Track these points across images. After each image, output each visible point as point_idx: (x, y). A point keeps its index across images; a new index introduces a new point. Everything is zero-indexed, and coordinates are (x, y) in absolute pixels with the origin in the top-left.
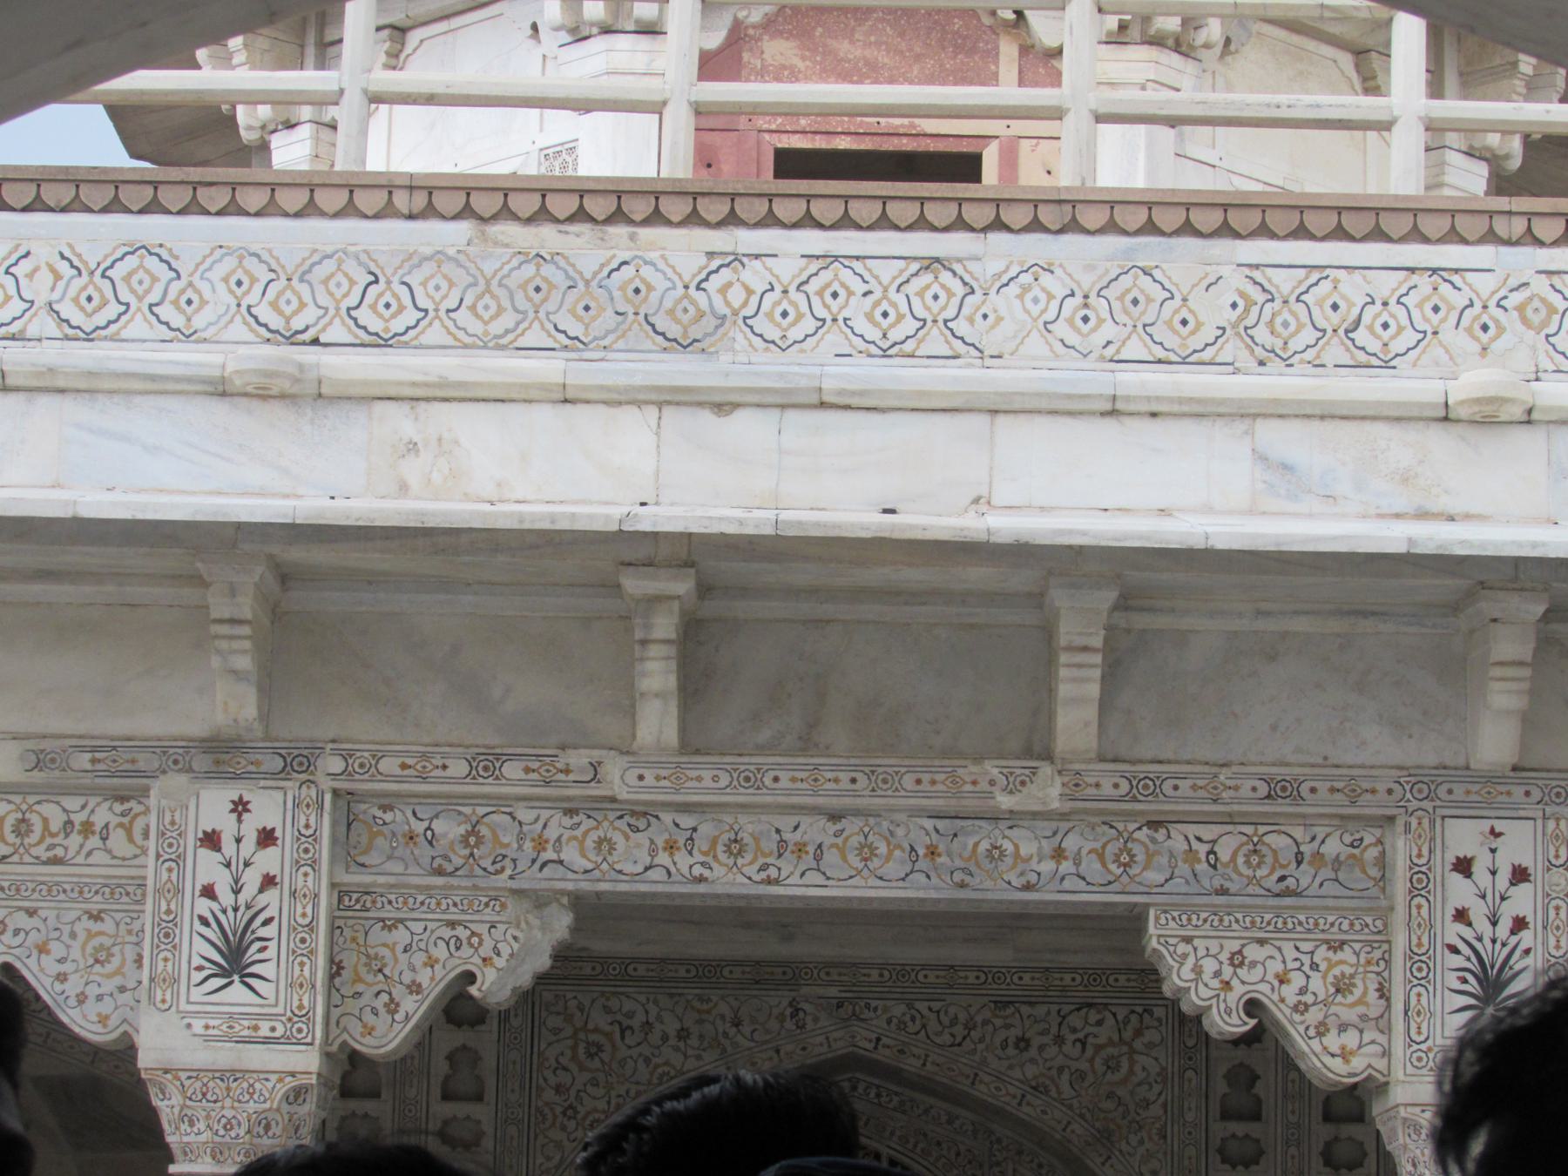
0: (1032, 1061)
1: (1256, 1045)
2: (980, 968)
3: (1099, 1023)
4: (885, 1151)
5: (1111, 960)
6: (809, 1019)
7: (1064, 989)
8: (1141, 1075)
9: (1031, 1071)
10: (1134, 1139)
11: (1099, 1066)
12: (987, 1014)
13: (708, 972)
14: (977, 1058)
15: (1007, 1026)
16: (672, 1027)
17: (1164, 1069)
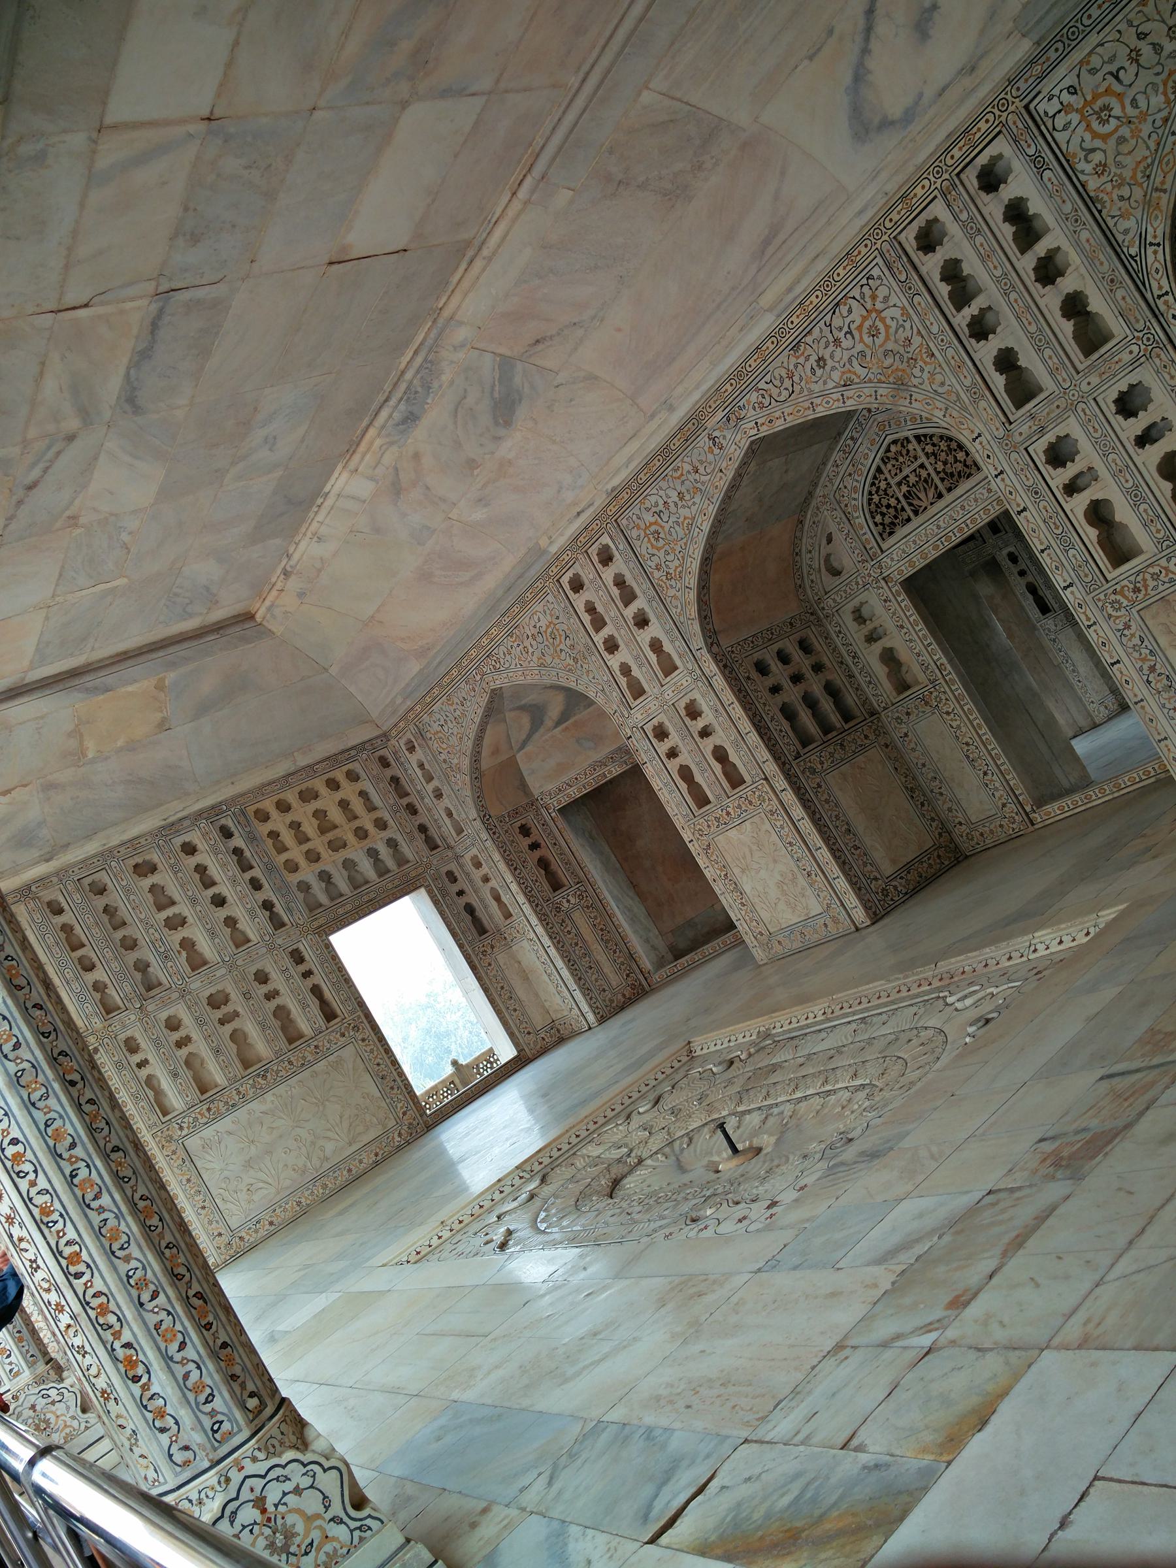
0: (833, 368)
1: (945, 240)
2: (770, 336)
3: (850, 311)
4: (909, 434)
5: (823, 265)
6: (722, 441)
7: (816, 308)
8: (893, 324)
9: (836, 375)
10: (916, 372)
11: (868, 340)
12: (793, 360)
13: (665, 454)
14: (806, 393)
15: (807, 358)
16: (674, 496)
17: (903, 308)
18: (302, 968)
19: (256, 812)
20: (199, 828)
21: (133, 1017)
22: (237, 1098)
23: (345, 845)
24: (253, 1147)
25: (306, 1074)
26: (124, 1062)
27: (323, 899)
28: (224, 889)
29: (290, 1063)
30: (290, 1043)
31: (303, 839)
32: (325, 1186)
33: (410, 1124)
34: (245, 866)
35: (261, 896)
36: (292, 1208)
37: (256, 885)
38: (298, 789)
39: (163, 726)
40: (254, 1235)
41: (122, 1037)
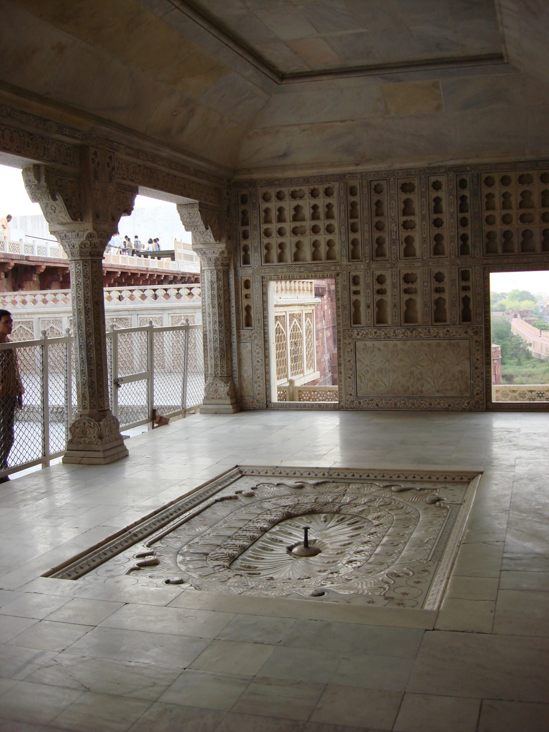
18: (463, 284)
19: (487, 179)
20: (448, 176)
21: (362, 266)
22: (392, 334)
23: (531, 221)
24: (387, 363)
25: (434, 342)
26: (348, 287)
27: (500, 250)
28: (445, 217)
29: (429, 332)
30: (437, 320)
31: (505, 205)
32: (413, 404)
33: (477, 401)
34: (463, 208)
35: (462, 231)
36: (391, 404)
37: (463, 223)
38: (520, 173)
39: (438, 108)
40: (366, 405)
41: (353, 274)
